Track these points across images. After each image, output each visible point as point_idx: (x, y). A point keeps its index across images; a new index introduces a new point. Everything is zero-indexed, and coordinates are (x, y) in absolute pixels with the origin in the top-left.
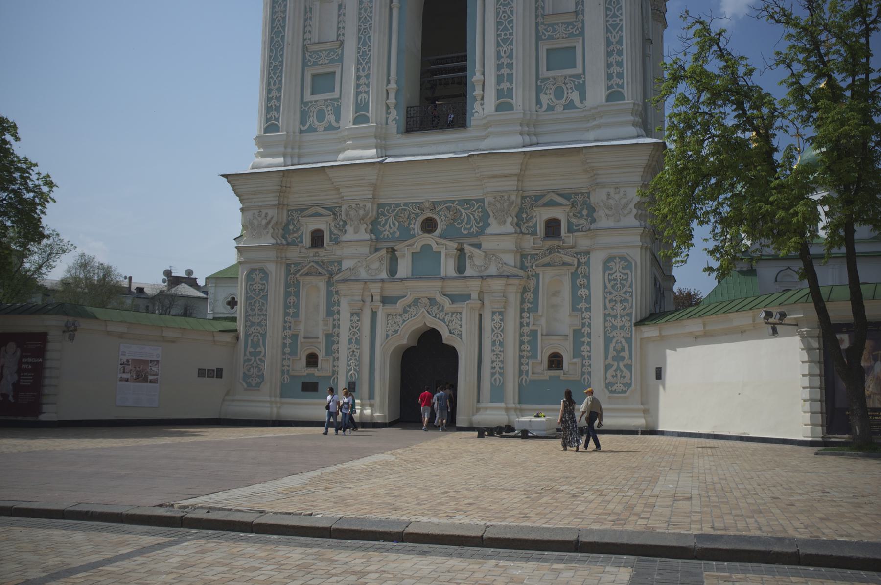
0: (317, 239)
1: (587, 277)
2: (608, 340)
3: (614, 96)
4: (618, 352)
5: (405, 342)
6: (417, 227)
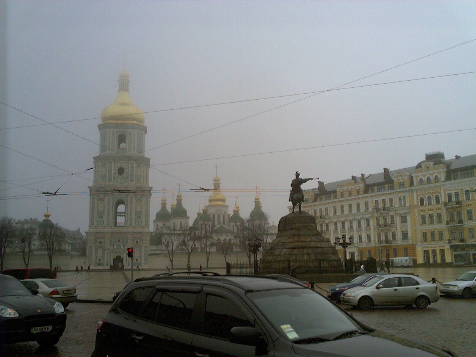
0: (100, 242)
1: (142, 249)
2: (144, 258)
3: (146, 224)
4: (146, 258)
5: (115, 258)
6: (117, 241)
